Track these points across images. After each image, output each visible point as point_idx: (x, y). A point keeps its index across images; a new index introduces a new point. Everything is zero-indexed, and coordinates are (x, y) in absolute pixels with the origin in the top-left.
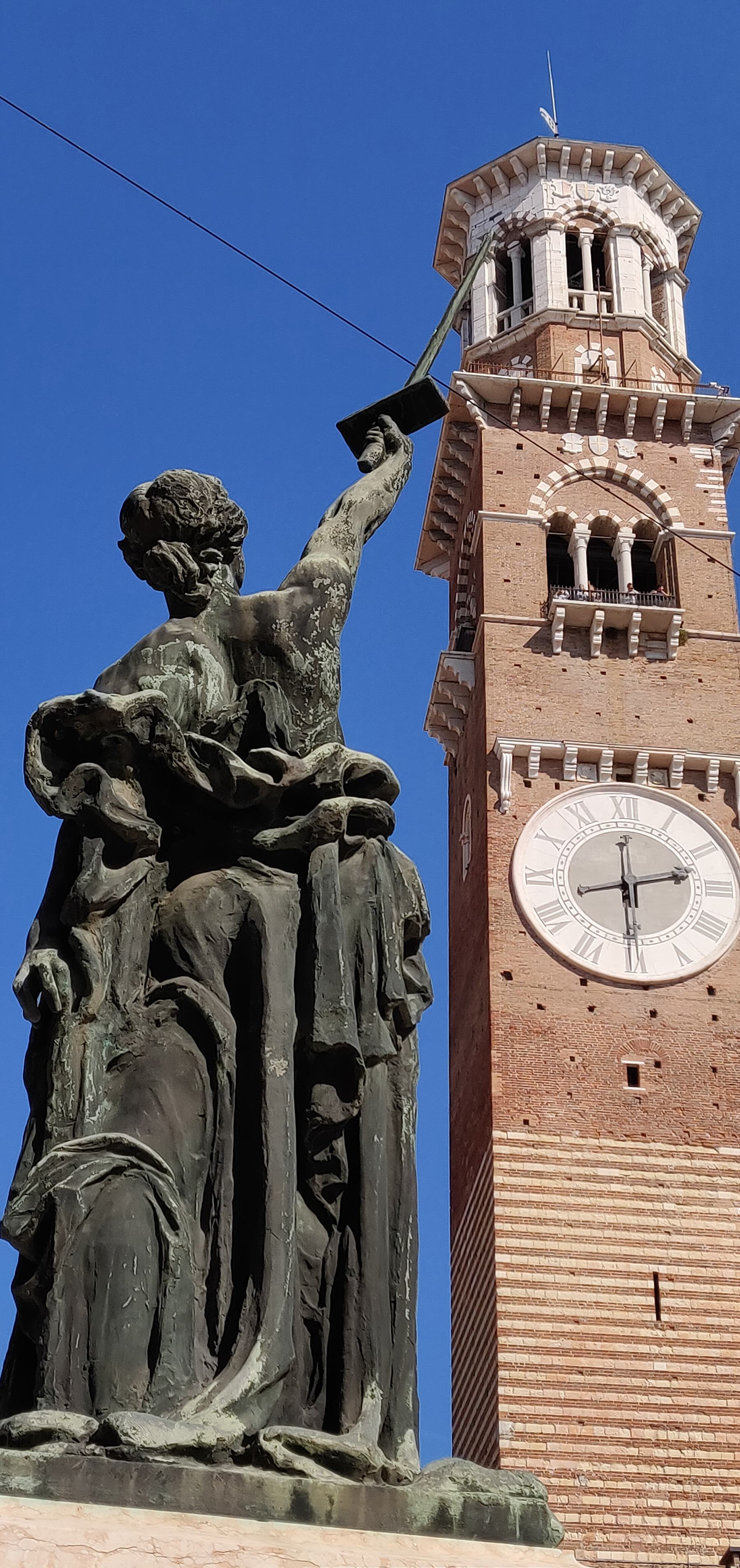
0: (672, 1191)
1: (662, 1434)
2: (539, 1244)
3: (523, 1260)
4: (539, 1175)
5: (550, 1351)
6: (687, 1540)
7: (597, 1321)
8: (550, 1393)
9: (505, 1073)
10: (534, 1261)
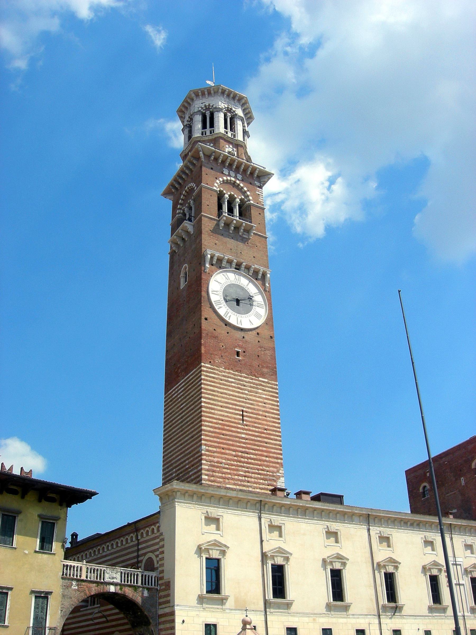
0: (247, 388)
1: (243, 455)
2: (213, 397)
3: (209, 401)
4: (214, 378)
5: (215, 428)
6: (249, 484)
7: (227, 421)
8: (215, 439)
9: (205, 347)
10: (212, 402)
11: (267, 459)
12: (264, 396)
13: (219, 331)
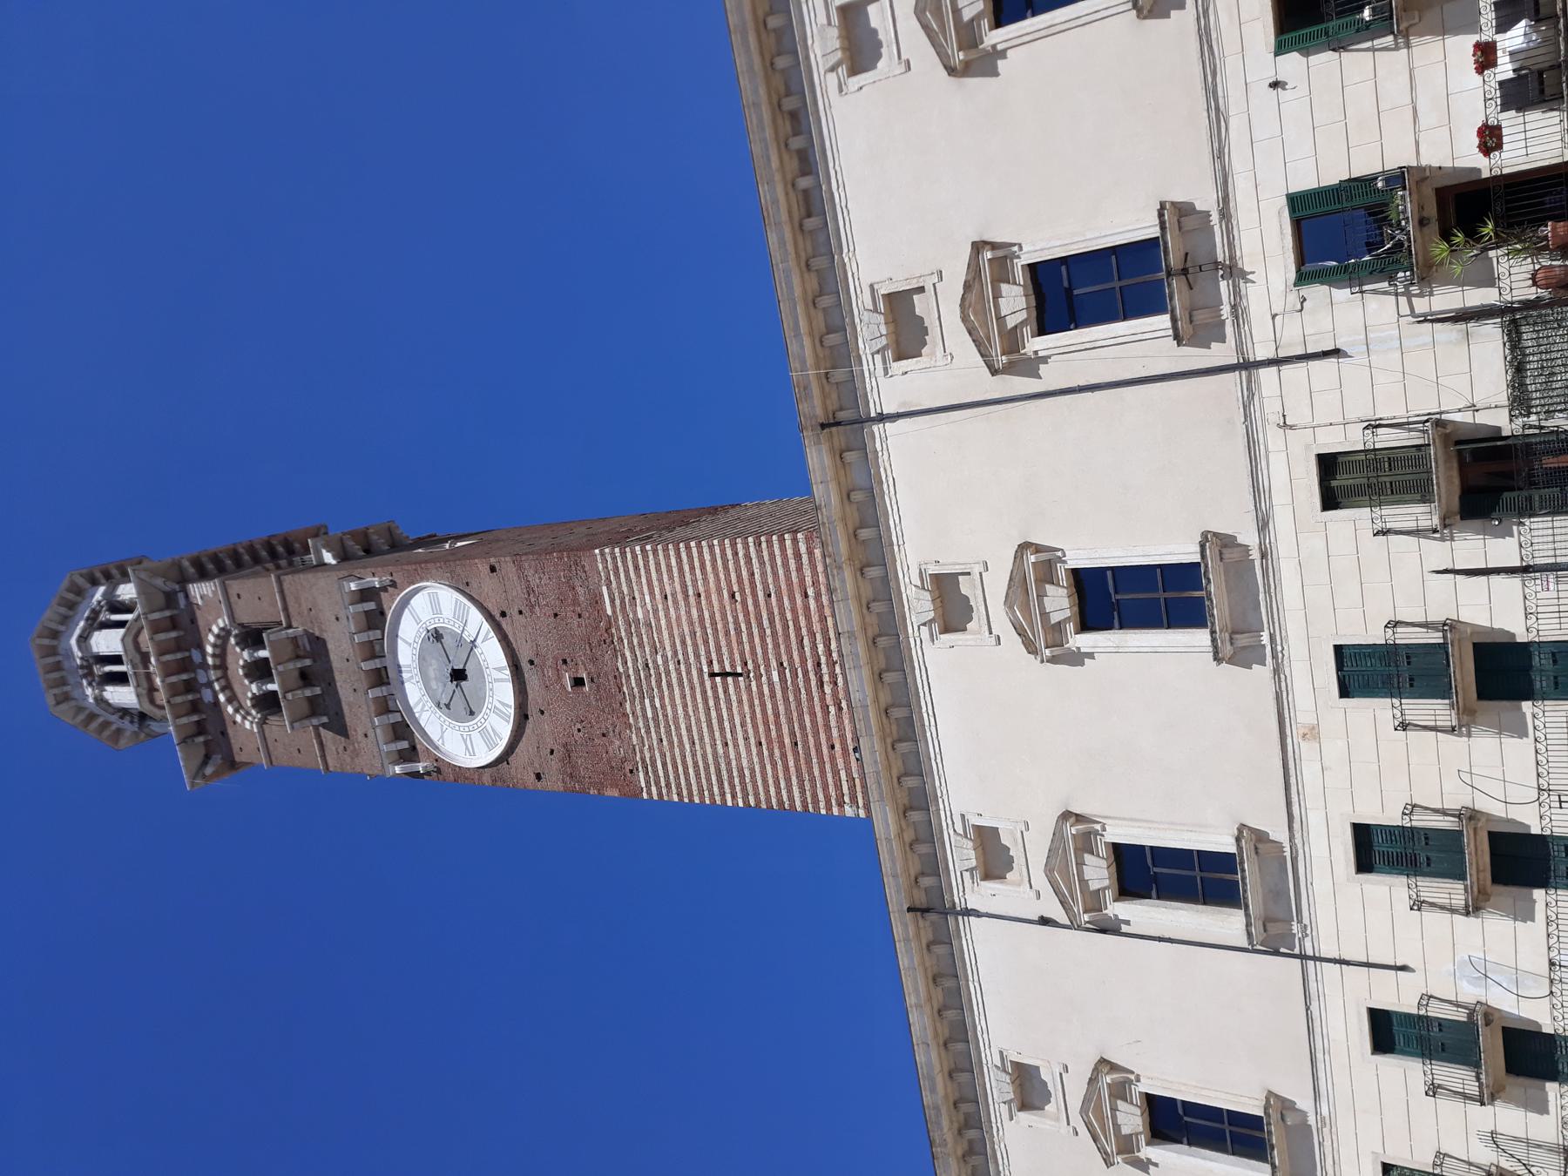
1: (826, 678)
4: (664, 764)
11: (810, 592)
12: (647, 598)
13: (550, 743)
